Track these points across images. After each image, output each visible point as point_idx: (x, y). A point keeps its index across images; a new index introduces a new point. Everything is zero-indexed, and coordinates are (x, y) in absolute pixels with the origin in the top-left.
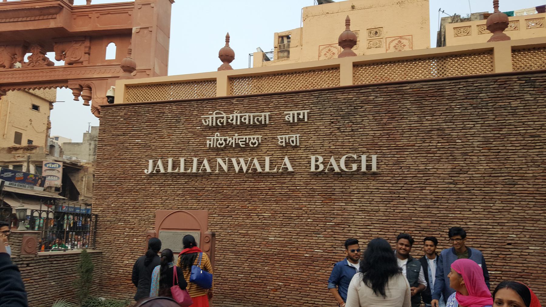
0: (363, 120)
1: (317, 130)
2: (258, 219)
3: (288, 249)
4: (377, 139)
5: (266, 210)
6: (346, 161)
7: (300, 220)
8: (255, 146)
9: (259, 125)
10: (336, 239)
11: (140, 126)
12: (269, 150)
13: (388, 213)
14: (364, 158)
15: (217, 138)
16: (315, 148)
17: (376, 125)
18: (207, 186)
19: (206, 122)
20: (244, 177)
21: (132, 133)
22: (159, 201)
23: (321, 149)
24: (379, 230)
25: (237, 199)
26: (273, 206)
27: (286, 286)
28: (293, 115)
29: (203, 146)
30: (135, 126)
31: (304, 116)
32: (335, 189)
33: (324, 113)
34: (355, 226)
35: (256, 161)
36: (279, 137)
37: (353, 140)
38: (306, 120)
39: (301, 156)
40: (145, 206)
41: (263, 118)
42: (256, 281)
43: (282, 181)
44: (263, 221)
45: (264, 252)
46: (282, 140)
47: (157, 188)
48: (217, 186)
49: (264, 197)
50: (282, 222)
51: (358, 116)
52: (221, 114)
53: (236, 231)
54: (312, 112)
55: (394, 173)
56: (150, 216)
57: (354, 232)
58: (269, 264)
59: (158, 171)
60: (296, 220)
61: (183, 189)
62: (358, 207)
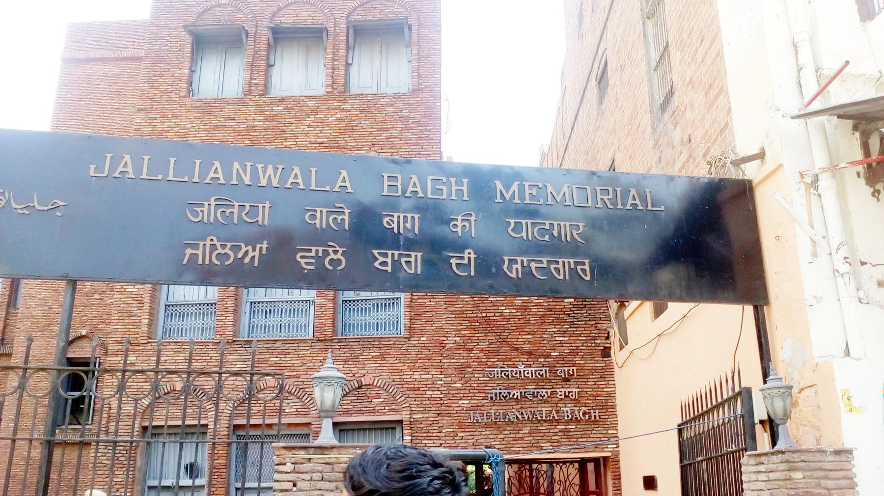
41: (544, 372)
46: (561, 393)
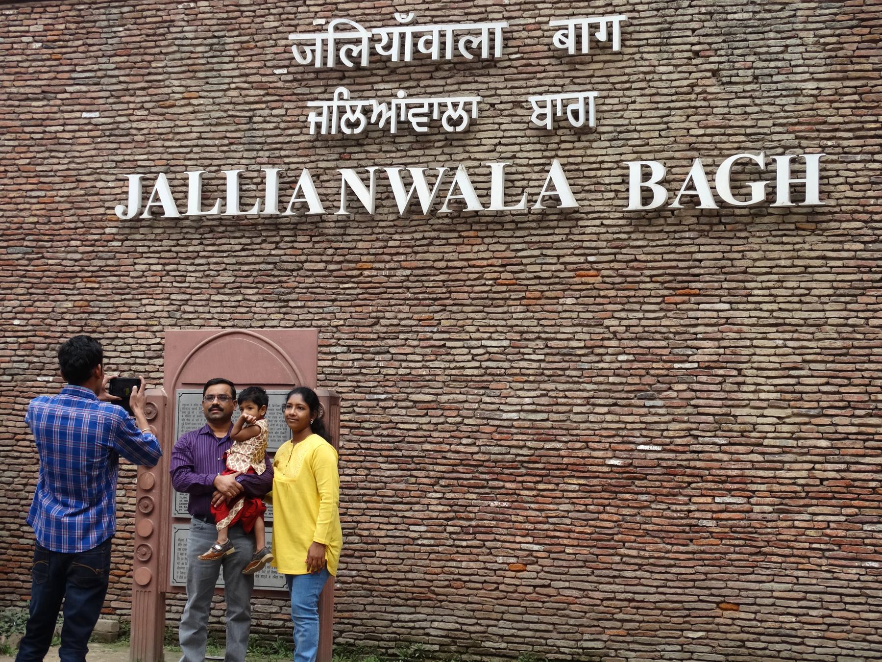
0: (787, 46)
1: (649, 77)
2: (469, 357)
3: (559, 445)
4: (826, 105)
5: (492, 329)
6: (733, 173)
7: (597, 358)
8: (460, 129)
9: (472, 62)
10: (701, 410)
11: (96, 67)
12: (503, 141)
13: (850, 329)
14: (783, 164)
15: (342, 103)
16: (643, 135)
17: (823, 62)
18: (310, 258)
19: (303, 53)
20: (427, 228)
21: (69, 89)
22: (160, 307)
23: (660, 136)
24: (824, 380)
25: (402, 296)
26: (515, 316)
27: (552, 555)
28: (578, 28)
29: (297, 131)
30: (78, 68)
31: (610, 34)
32: (700, 261)
33: (672, 23)
34: (754, 372)
35: (462, 178)
36: (533, 99)
37: (757, 109)
38: (616, 47)
39: (600, 159)
40: (119, 323)
41: (485, 38)
42: (464, 543)
43: (542, 239)
44: (485, 364)
45: (487, 457)
46: (542, 111)
47: (153, 267)
48: (341, 258)
49: (487, 288)
50: (543, 365)
51: (772, 35)
52: (353, 28)
53: (404, 396)
54: (635, 22)
55: (870, 209)
56: (134, 354)
57: (752, 388)
58: (503, 491)
59: (157, 212)
60: (583, 359)
61: (236, 267)
62: (766, 314)
